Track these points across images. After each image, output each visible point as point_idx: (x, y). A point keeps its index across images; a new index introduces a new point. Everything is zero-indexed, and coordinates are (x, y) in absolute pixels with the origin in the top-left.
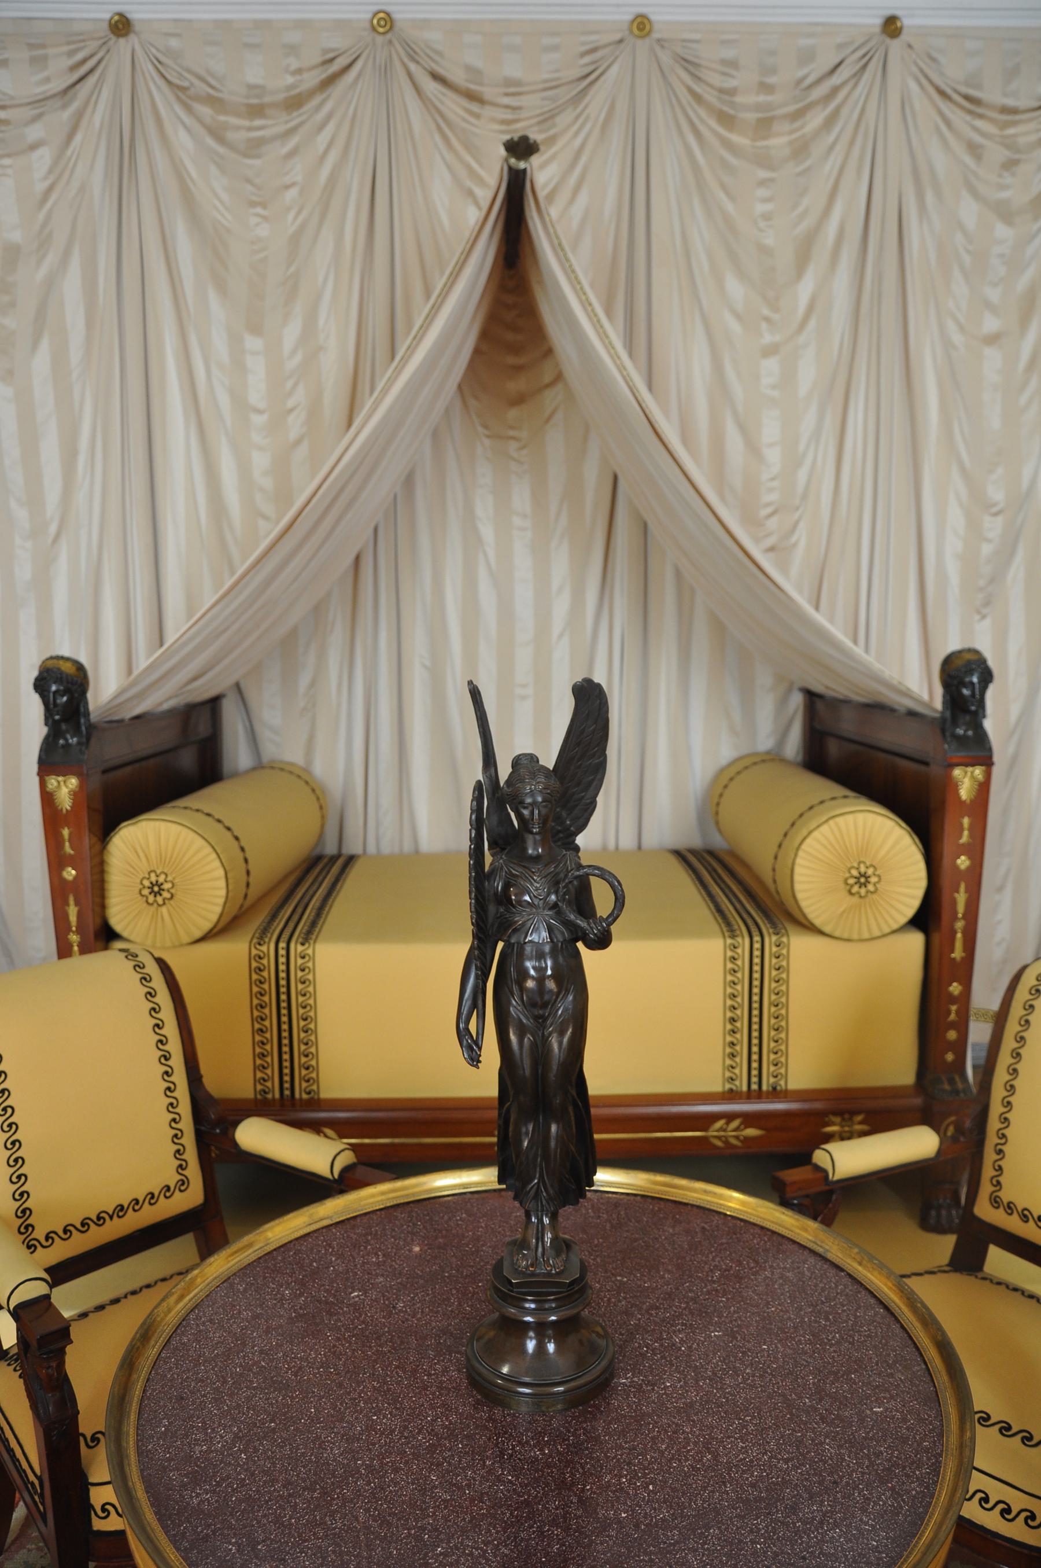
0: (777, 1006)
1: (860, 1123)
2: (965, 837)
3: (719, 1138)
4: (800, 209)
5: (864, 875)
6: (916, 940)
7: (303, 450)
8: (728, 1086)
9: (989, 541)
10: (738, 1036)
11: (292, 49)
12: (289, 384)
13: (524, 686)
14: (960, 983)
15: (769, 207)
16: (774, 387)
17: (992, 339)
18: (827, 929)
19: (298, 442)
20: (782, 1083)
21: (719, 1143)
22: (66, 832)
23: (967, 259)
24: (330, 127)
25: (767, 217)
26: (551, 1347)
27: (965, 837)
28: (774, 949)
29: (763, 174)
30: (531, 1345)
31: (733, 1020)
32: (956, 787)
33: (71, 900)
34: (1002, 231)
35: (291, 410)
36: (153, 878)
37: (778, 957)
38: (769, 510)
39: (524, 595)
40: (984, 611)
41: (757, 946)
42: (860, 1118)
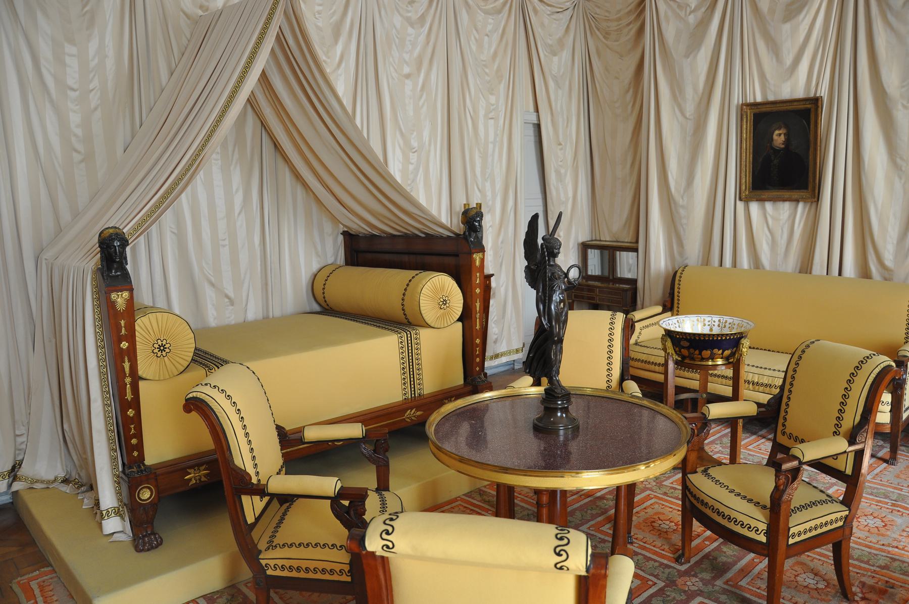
3: (408, 418)
4: (333, 10)
5: (445, 300)
6: (460, 324)
7: (98, 114)
8: (404, 397)
9: (412, 164)
10: (406, 375)
12: (91, 75)
15: (321, 8)
17: (408, 76)
18: (432, 325)
19: (96, 109)
20: (422, 392)
21: (409, 420)
22: (123, 323)
23: (397, 40)
25: (319, 13)
26: (564, 415)
30: (559, 414)
31: (403, 368)
32: (475, 261)
33: (126, 359)
34: (410, 30)
35: (92, 90)
36: (160, 343)
39: (219, 193)
41: (409, 335)
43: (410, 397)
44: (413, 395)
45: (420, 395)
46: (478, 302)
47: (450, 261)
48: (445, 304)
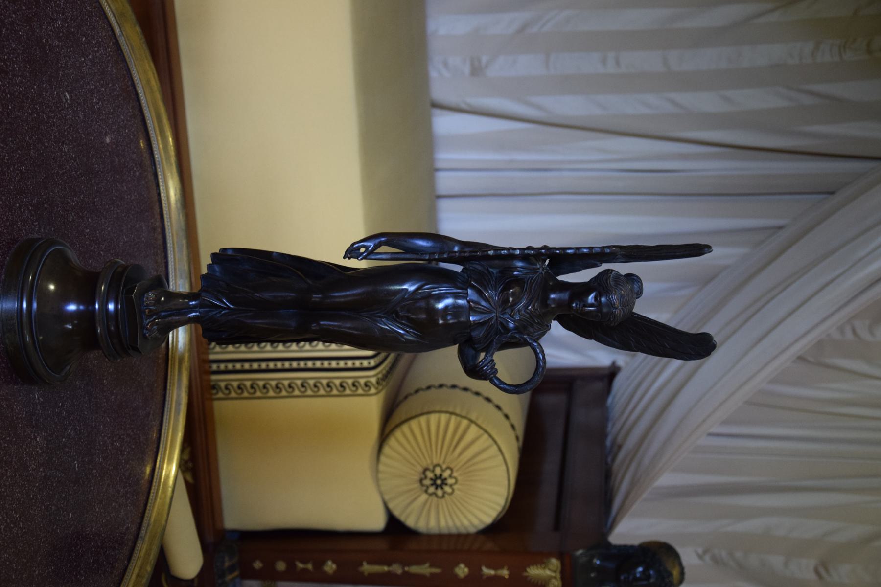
0: (303, 386)
2: (487, 571)
6: (377, 523)
9: (786, 564)
13: (618, 63)
14: (335, 572)
20: (220, 395)
27: (487, 571)
28: (362, 381)
37: (354, 385)
40: (707, 558)
41: (365, 363)
43: (212, 357)
44: (214, 367)
45: (214, 387)
47: (544, 519)
48: (434, 484)
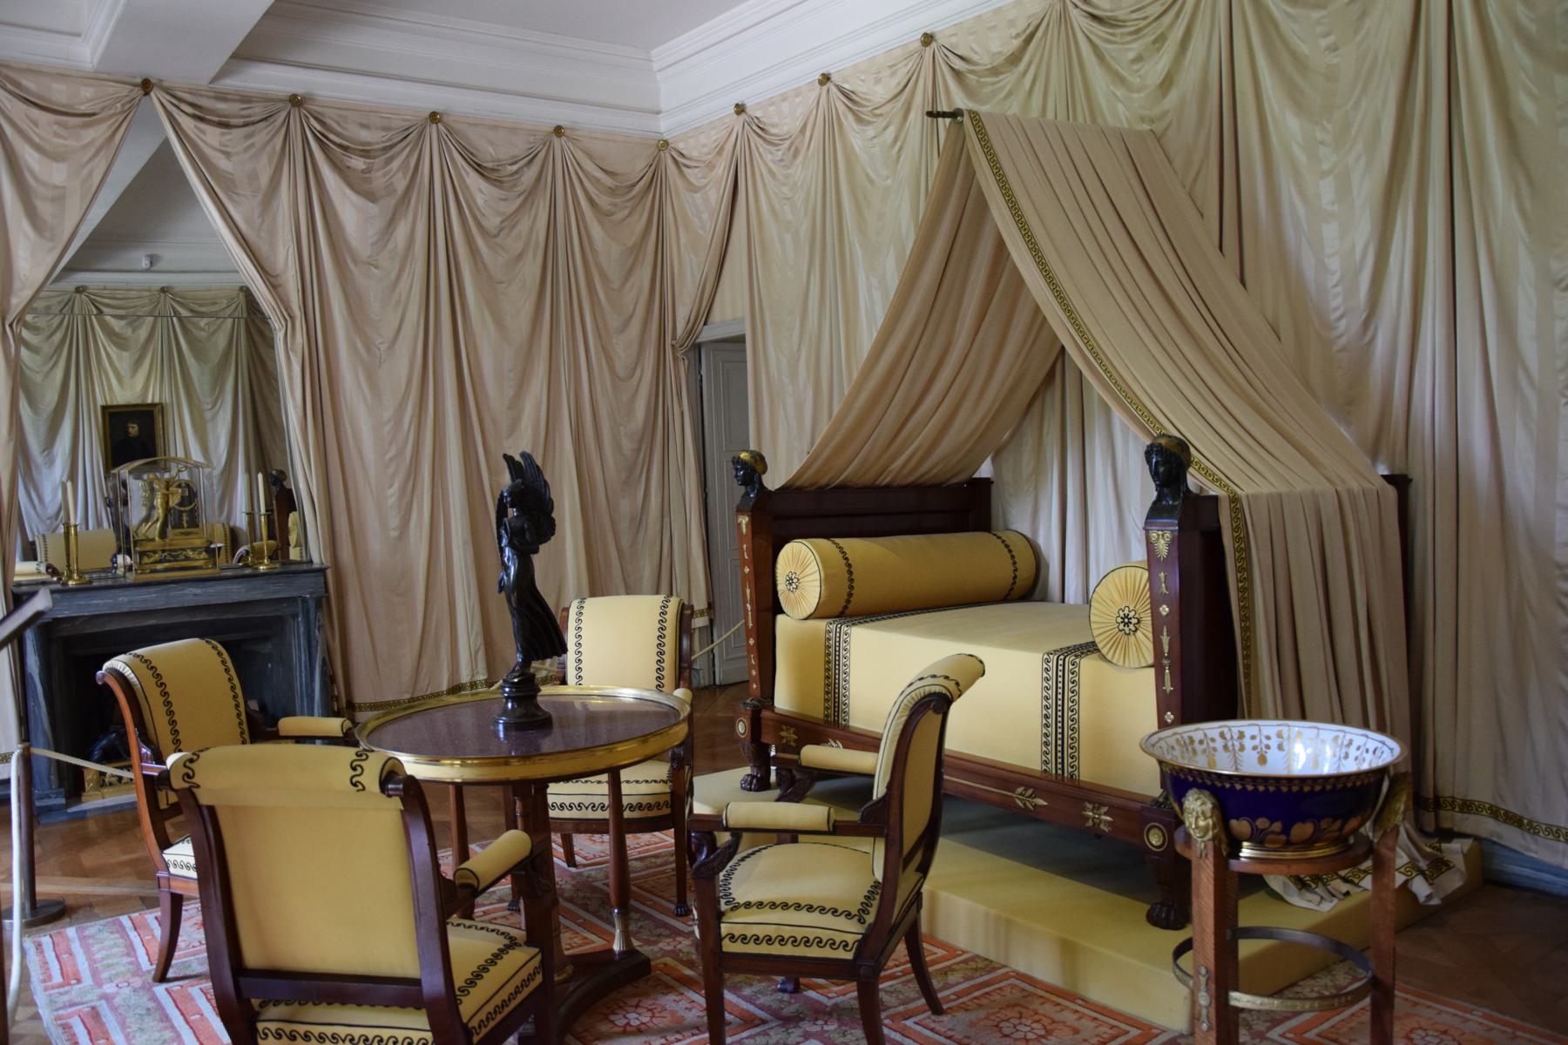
1: (1105, 814)
8: (1044, 767)
11: (1012, 23)
15: (1332, 39)
16: (1333, 203)
20: (1076, 773)
24: (1033, 68)
29: (1316, 15)
38: (1337, 314)
42: (1105, 809)
44: (1060, 772)
45: (1072, 776)
46: (1165, 633)
